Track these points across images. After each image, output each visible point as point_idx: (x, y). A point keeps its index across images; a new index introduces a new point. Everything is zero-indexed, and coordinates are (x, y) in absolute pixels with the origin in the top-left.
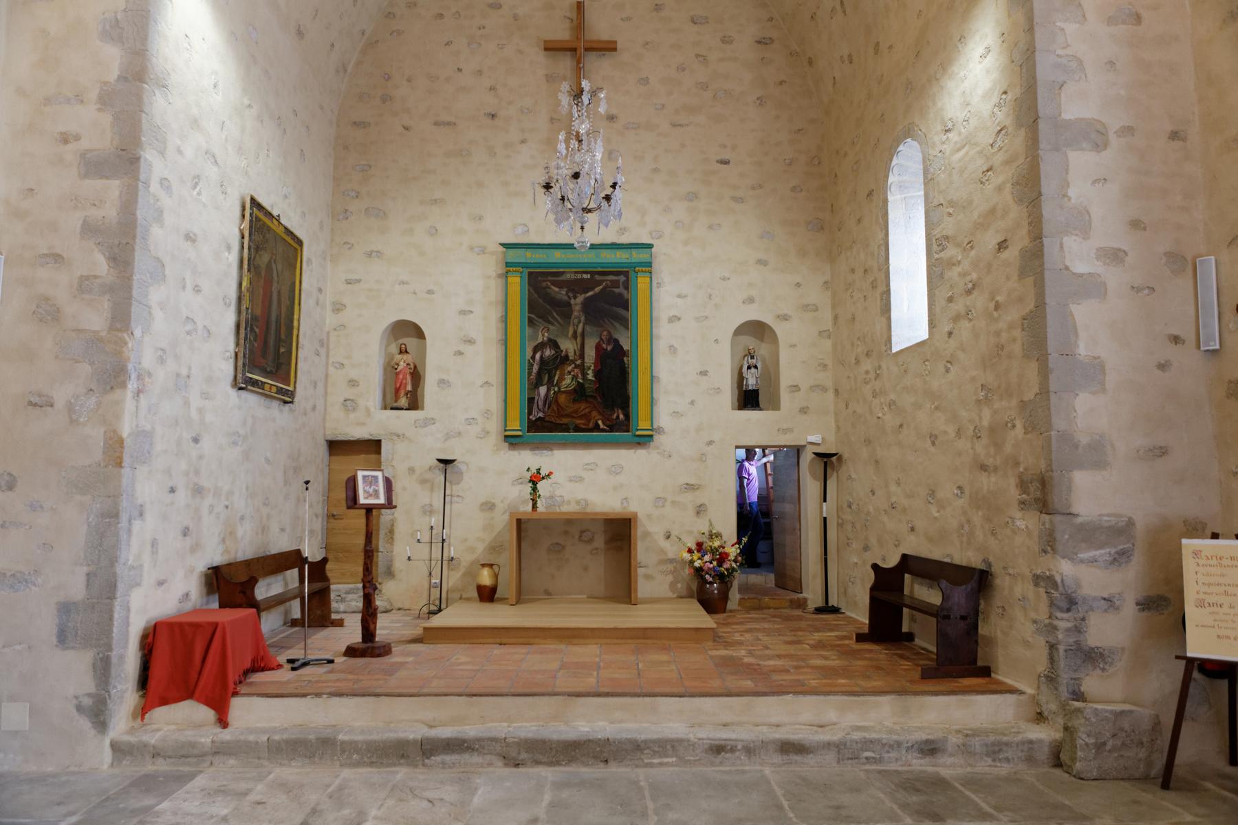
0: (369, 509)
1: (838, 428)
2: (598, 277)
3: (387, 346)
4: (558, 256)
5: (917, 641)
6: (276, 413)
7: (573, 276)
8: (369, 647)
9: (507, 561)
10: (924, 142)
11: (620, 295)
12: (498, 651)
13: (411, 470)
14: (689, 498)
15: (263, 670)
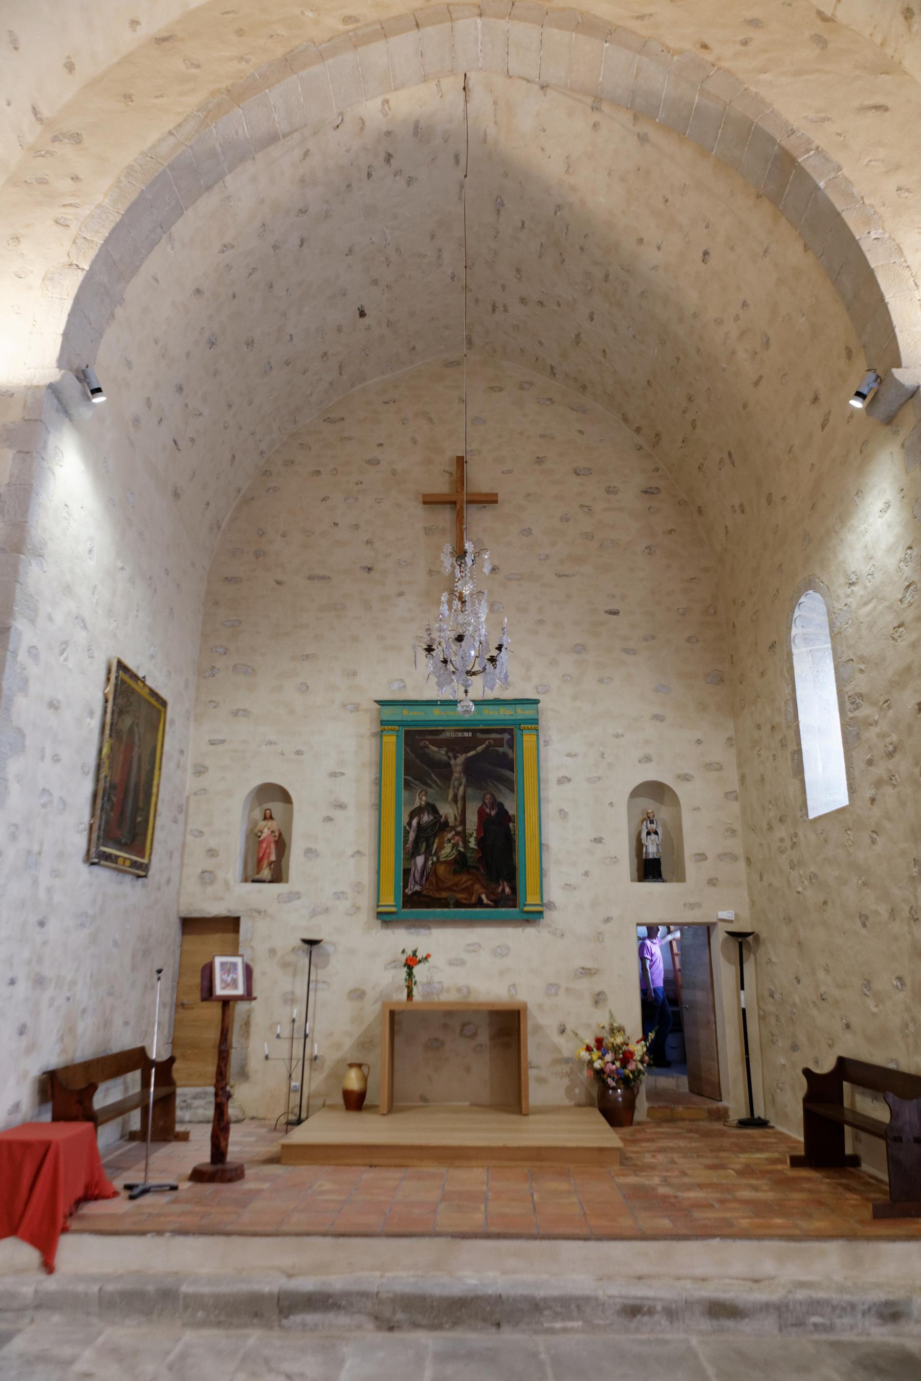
0: (226, 1003)
1: (753, 903)
2: (479, 735)
3: (251, 810)
4: (436, 714)
5: (865, 1167)
6: (128, 890)
7: (453, 735)
8: (218, 1170)
9: (378, 1059)
10: (827, 595)
11: (505, 755)
12: (368, 1175)
13: (272, 952)
14: (584, 985)
15: (96, 1198)
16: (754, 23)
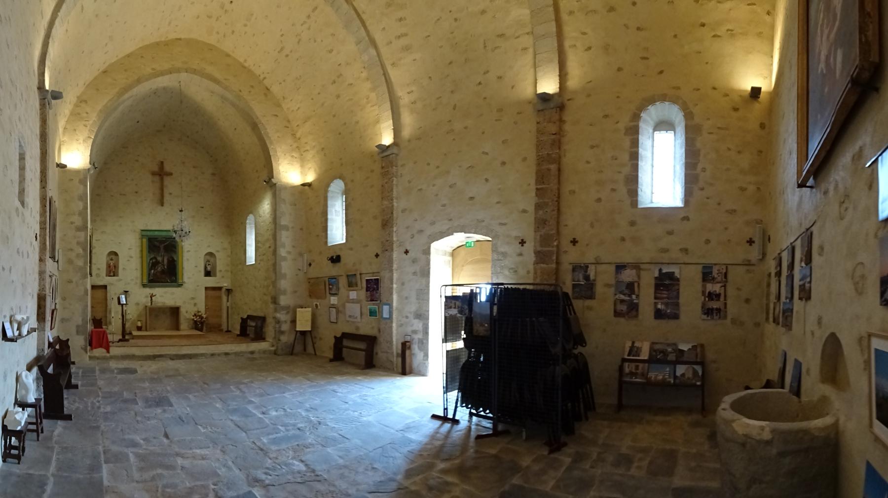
16: (252, 87)
